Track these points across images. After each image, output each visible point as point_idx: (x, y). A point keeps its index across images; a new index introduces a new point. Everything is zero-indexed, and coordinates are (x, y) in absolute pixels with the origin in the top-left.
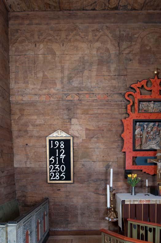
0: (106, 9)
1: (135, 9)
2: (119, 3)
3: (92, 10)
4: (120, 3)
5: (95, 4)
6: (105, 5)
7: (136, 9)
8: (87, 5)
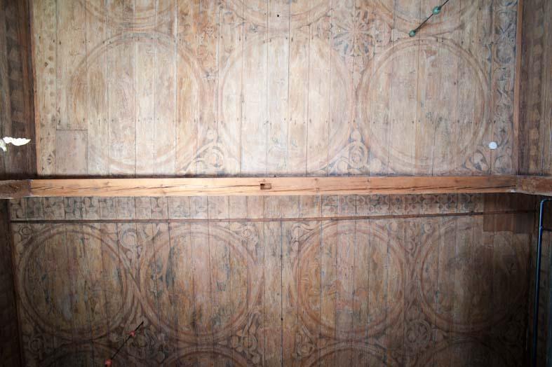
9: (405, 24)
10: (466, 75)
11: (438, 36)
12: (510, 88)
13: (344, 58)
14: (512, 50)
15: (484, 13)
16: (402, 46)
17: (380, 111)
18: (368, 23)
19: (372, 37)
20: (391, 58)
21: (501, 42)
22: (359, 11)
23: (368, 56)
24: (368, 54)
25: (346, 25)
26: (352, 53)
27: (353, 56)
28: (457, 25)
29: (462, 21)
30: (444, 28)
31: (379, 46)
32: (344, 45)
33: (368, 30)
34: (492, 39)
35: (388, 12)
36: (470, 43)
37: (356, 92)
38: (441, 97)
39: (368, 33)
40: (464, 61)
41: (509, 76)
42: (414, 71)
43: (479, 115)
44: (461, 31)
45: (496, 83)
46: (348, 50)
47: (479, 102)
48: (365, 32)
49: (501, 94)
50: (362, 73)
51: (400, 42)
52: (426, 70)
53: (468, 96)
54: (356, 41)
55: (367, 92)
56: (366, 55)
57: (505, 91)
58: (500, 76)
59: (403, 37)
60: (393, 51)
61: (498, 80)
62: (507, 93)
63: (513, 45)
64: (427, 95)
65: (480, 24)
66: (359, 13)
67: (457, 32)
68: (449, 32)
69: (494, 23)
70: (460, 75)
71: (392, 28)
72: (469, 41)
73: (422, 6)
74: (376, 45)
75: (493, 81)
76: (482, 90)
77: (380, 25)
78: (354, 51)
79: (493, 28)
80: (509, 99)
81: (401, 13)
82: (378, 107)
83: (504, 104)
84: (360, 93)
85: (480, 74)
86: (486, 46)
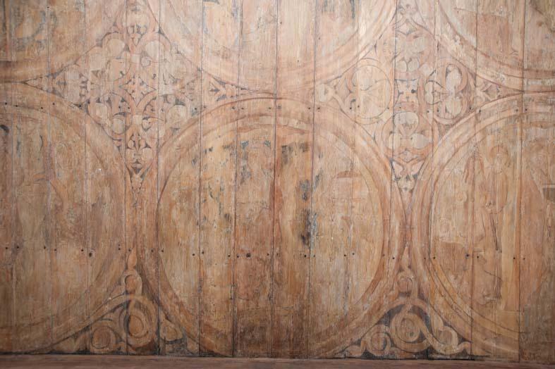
0: (123, 350)
1: (212, 354)
2: (158, 333)
3: (79, 352)
4: (161, 331)
5: (87, 333)
6: (117, 335)
7: (215, 350)
8: (63, 338)
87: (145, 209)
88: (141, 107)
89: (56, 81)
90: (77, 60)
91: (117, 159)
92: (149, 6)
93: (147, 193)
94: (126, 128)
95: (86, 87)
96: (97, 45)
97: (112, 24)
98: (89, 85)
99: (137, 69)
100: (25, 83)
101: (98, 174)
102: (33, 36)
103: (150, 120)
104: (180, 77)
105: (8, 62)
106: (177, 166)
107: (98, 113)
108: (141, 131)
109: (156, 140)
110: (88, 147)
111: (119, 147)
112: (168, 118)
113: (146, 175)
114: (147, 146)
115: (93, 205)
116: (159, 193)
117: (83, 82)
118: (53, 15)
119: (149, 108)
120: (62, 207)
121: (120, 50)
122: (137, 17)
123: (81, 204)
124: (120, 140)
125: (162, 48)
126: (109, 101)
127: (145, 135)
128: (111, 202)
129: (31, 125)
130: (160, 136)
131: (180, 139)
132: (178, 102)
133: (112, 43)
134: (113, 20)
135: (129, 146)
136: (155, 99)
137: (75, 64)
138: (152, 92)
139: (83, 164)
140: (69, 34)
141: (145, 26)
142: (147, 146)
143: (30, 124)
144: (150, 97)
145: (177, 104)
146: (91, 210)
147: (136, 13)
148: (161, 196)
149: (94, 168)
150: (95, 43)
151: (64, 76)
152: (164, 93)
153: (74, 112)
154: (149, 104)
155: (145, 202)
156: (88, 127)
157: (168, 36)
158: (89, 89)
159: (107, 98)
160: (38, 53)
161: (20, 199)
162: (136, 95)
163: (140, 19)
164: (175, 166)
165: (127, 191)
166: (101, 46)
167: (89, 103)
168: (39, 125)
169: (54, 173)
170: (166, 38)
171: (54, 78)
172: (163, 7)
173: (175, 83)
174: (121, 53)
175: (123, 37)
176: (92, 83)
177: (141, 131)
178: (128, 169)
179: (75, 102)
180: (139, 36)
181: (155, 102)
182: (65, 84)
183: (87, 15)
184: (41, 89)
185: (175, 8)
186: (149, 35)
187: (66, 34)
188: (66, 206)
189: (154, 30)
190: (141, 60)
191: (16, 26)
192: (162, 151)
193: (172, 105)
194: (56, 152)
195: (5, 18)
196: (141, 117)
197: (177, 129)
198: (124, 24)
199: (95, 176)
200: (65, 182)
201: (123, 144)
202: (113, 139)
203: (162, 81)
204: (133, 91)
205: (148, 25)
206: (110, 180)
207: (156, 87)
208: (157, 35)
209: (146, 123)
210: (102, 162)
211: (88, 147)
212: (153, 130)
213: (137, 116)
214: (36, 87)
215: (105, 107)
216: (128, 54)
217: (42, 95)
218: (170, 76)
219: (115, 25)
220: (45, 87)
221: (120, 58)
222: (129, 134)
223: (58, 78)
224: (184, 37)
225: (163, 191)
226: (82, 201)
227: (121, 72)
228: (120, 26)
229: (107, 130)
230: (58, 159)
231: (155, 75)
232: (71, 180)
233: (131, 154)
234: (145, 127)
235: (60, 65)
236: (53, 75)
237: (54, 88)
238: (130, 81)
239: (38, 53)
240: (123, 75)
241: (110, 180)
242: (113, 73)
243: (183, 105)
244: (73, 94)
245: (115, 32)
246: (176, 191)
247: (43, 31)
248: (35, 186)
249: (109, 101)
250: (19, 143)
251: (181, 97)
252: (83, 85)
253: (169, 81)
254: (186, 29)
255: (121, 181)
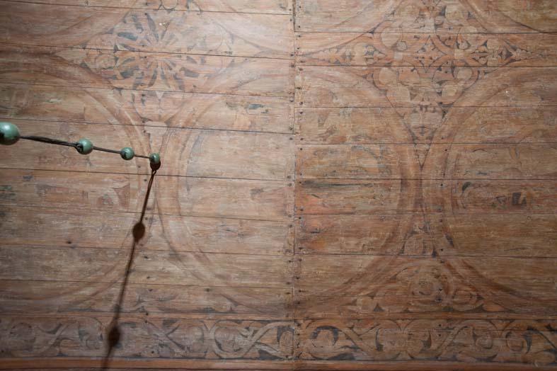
9: (176, 148)
10: (86, 265)
11: (156, 211)
12: (64, 350)
13: (111, 32)
14: (137, 352)
15: (201, 297)
16: (135, 141)
17: (14, 98)
18: (176, 79)
19: (151, 85)
20: (114, 121)
21: (149, 331)
22: (199, 62)
23: (115, 77)
24: (119, 77)
25: (171, 37)
26: (119, 47)
27: (116, 50)
28: (177, 246)
29: (184, 256)
30: (171, 222)
31: (133, 96)
32: (136, 32)
33: (164, 77)
34: (155, 313)
35: (197, 114)
36: (146, 272)
37: (48, 54)
38: (42, 216)
39: (159, 78)
40: (112, 260)
41: (89, 348)
42: (91, 164)
43: (11, 289)
44: (166, 254)
45: (73, 322)
46: (126, 41)
47: (35, 289)
48: (159, 73)
49: (54, 332)
50: (84, 67)
51: (142, 138)
52: (92, 187)
53: (46, 269)
54: (143, 54)
55: (48, 74)
56: (118, 73)
57: (59, 340)
58: (88, 328)
59: (152, 145)
60: (126, 124)
61: (79, 326)
62: (57, 344)
63: (145, 354)
64: (46, 187)
65: (179, 291)
66: (194, 62)
67: (165, 246)
68: (163, 231)
69: (182, 316)
70: (87, 251)
71: (169, 123)
72: (150, 269)
73: (209, 180)
74: (136, 93)
75: (77, 316)
76: (59, 295)
77: (174, 101)
78: (125, 52)
79: (173, 316)
80: (46, 348)
81: (196, 141)
82: (20, 95)
83: (34, 340)
84: (46, 61)
85: (88, 291)
86: (140, 301)
87: (547, 46)
88: (447, 50)
89: (420, 136)
90: (400, 116)
91: (497, 76)
92: (346, 43)
93: (532, 45)
94: (467, 66)
95: (426, 107)
96: (385, 94)
97: (365, 80)
98: (424, 104)
99: (409, 54)
100: (422, 166)
101: (512, 94)
102: (377, 158)
103: (459, 42)
104: (417, 10)
105: (402, 183)
106: (506, 13)
107: (452, 94)
108: (470, 50)
109: (480, 35)
110: (484, 105)
111: (486, 73)
112: (457, 23)
113: (513, 45)
114: (485, 44)
115: (543, 99)
116: (533, 32)
117: (421, 109)
118: (356, 138)
119: (448, 43)
120: (543, 131)
121: (390, 71)
122: (357, 55)
123: (540, 111)
124: (479, 72)
125: (388, 29)
126: (441, 83)
127: (474, 46)
128: (539, 81)
129: (463, 161)
130: (476, 31)
131: (479, 11)
132: (442, 14)
133: (384, 81)
134: (362, 79)
135: (484, 62)
136: (438, 37)
137: (403, 117)
138: (432, 40)
139: (501, 109)
140: (374, 123)
141: (366, 47)
142: (485, 44)
143: (461, 162)
144: (437, 42)
145: (444, 15)
146: (547, 101)
147: (354, 56)
148: (535, 30)
149: (507, 98)
150: (383, 97)
151: (416, 128)
152: (433, 27)
153: (450, 119)
154: (444, 43)
155: (541, 46)
156: (465, 104)
157: (377, 24)
158: (428, 103)
159: (437, 85)
160: (392, 153)
161: (534, 172)
162: (435, 55)
163: (359, 51)
164: (507, 16)
165: (529, 65)
166: (386, 90)
167: (441, 103)
168: (463, 153)
169: (509, 138)
170: (378, 26)
171: (417, 138)
172: (347, 29)
173: (423, 17)
174: (393, 71)
175: (377, 69)
176: (423, 100)
177: (470, 50)
178: (507, 64)
179: (441, 117)
180: (376, 53)
181: (442, 36)
182: (423, 127)
183: (356, 105)
184: (428, 150)
185: (348, 17)
186: (375, 43)
187: (374, 126)
188: (542, 126)
189: (371, 38)
190: (400, 51)
191: (367, 174)
192: (491, 29)
193: (445, 19)
194: (489, 137)
195: (360, 184)
196: (457, 50)
197: (469, 14)
198: (364, 68)
199: (514, 97)
200: (519, 127)
201: (482, 69)
202: (477, 79)
203: (421, 30)
204: (431, 58)
205: (365, 44)
206: (518, 82)
207: (428, 35)
208: (375, 35)
209: (463, 45)
210: (500, 90)
211: (484, 105)
212: (469, 37)
213: (455, 54)
214: (426, 155)
215: (446, 87)
216: (395, 64)
217: (434, 150)
218: (416, 21)
219: (365, 77)
220: (426, 147)
221: (398, 72)
222: (472, 63)
223: (417, 135)
224: (377, 7)
225: (530, 28)
226: (537, 110)
227: (412, 71)
228: (366, 72)
229: (468, 85)
230: (496, 135)
231: (415, 37)
232: (517, 122)
233: (493, 60)
234: (466, 47)
235: (405, 132)
236: (413, 140)
237: (427, 139)
238: (420, 61)
239: (392, 153)
240: (415, 69)
241: (518, 82)
242: (413, 80)
243: (445, 8)
244: (433, 119)
245: (372, 76)
246: (531, 14)
247: (372, 148)
248: (522, 157)
249: (441, 83)
250: (480, 173)
251: (438, 10)
252: (424, 109)
253: (421, 22)
254: (369, 6)
255: (519, 71)
